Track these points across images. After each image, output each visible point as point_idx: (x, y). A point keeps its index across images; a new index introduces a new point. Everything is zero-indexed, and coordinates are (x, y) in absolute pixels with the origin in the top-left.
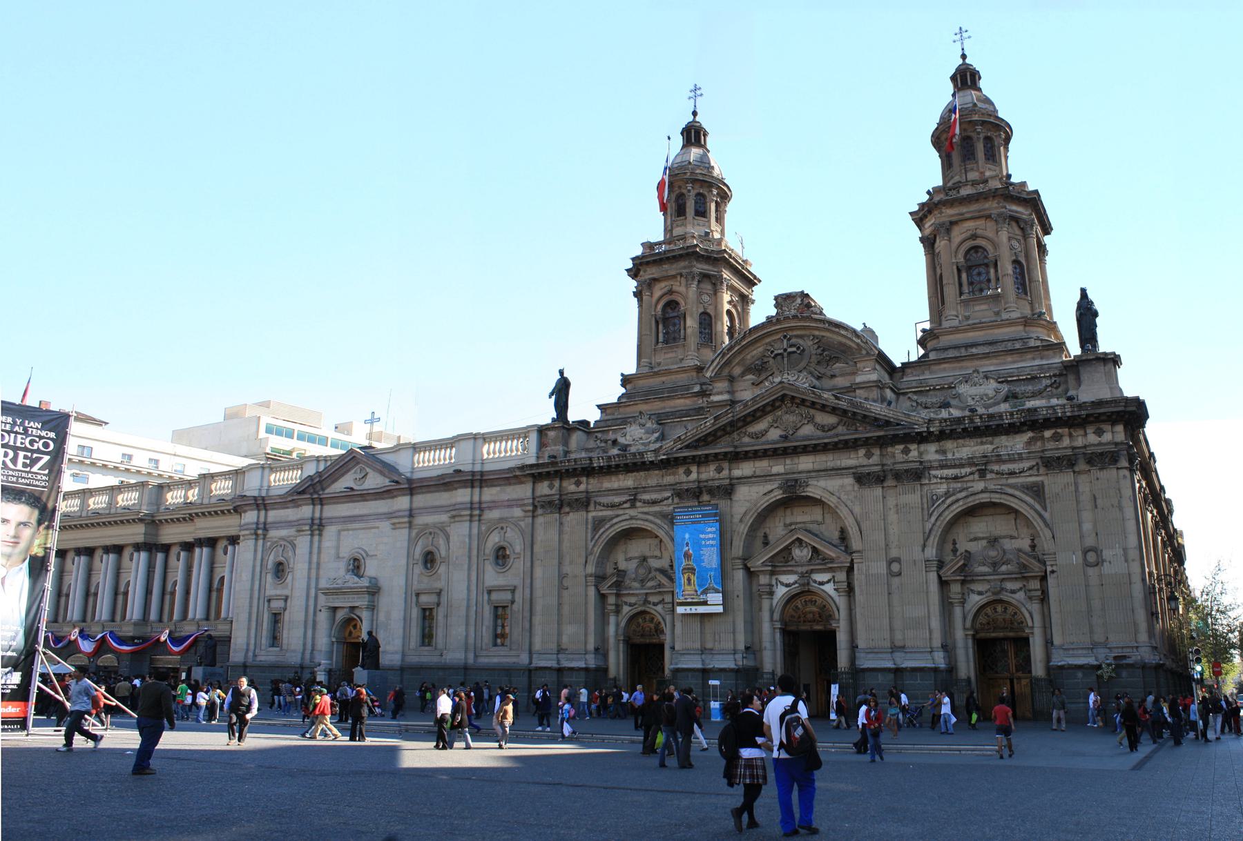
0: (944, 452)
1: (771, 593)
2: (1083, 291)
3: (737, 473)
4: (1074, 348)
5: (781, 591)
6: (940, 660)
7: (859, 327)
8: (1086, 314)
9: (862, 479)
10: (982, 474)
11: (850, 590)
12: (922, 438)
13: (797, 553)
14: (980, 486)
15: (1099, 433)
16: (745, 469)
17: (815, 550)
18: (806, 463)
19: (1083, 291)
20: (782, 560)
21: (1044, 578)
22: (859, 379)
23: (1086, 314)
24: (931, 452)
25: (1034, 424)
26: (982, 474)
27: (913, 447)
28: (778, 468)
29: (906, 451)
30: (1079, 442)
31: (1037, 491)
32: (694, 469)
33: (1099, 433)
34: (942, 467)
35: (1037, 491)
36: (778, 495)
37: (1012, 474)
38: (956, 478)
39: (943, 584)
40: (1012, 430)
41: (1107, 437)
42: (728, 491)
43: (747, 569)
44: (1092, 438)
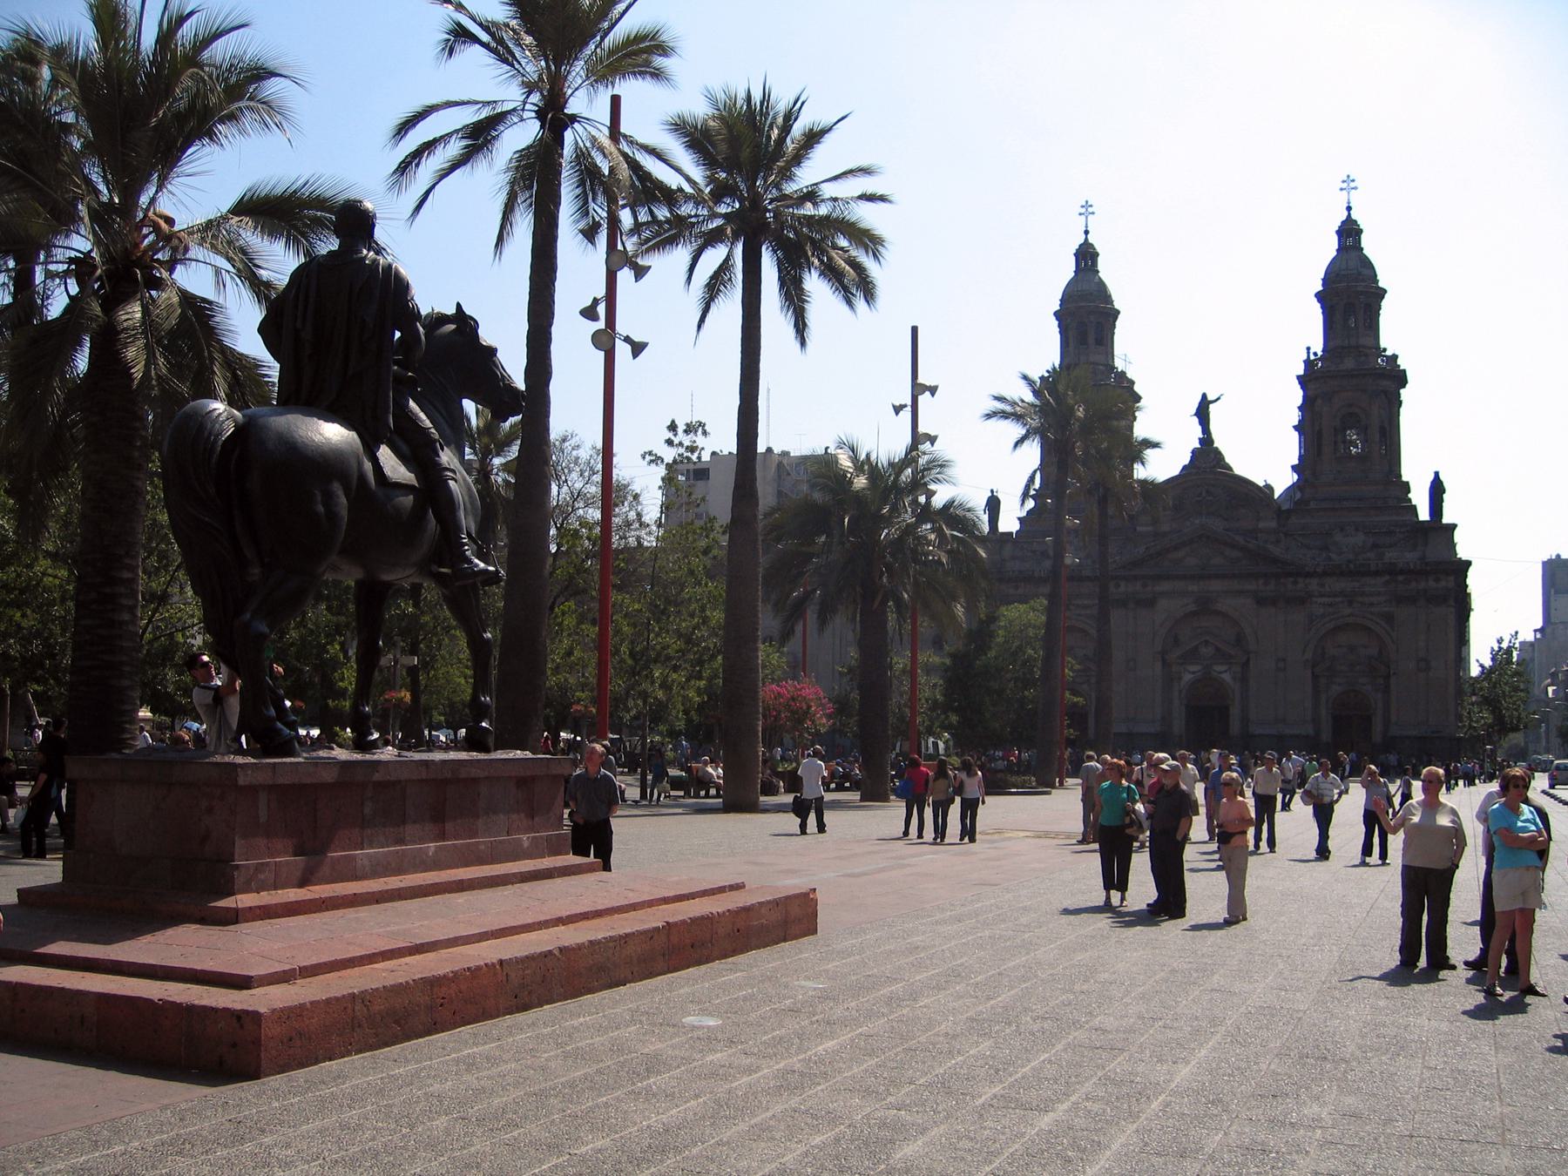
0: (1323, 585)
1: (1180, 679)
2: (1437, 474)
3: (1158, 588)
4: (1424, 514)
5: (1187, 677)
6: (1311, 731)
7: (1261, 484)
8: (1437, 490)
9: (1261, 601)
10: (1350, 603)
11: (1244, 679)
12: (1308, 575)
13: (1204, 650)
14: (1348, 611)
15: (1437, 580)
16: (1165, 586)
17: (1217, 649)
18: (1216, 586)
19: (1437, 474)
20: (1192, 656)
21: (1388, 677)
22: (1261, 525)
23: (1437, 490)
24: (1314, 584)
25: (1392, 571)
26: (1350, 603)
27: (1300, 580)
28: (1193, 588)
29: (1295, 583)
30: (1422, 585)
31: (1389, 618)
32: (1123, 584)
33: (1437, 580)
34: (1322, 596)
35: (1389, 618)
36: (1192, 608)
37: (1372, 604)
38: (1330, 605)
39: (1315, 677)
40: (1377, 573)
41: (1443, 583)
42: (1150, 603)
43: (1164, 661)
44: (1432, 583)
